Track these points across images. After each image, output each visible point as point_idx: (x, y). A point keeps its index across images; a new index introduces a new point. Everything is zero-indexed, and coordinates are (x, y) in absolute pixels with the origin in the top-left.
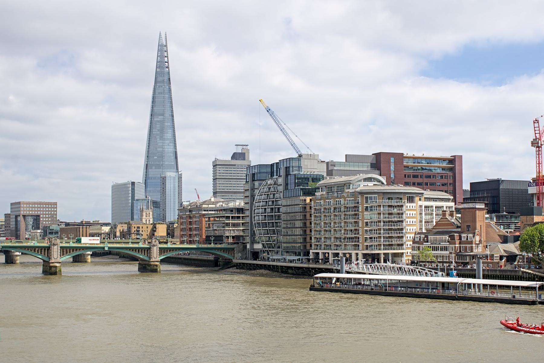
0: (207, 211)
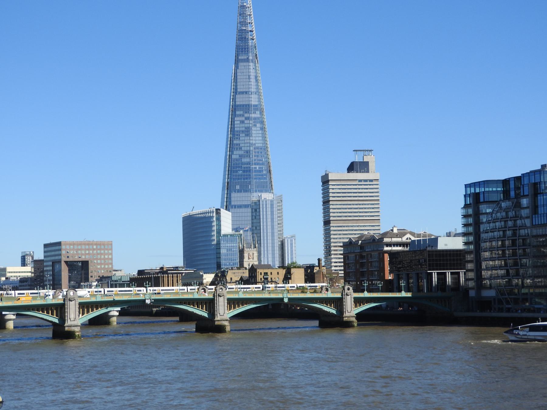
0: (390, 246)
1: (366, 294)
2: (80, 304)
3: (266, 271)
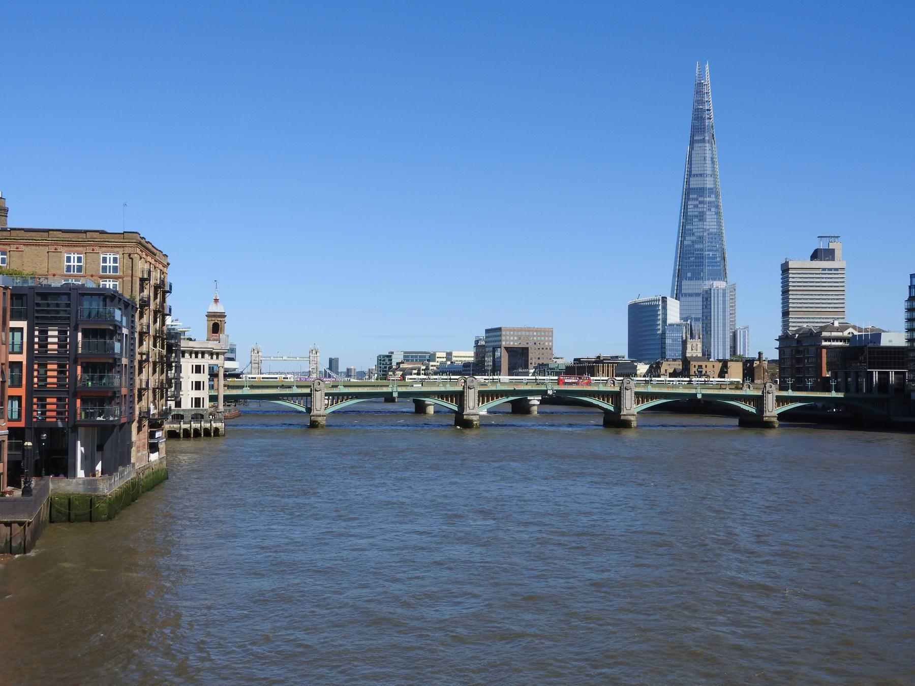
1: (790, 393)
2: (480, 392)
3: (700, 363)
